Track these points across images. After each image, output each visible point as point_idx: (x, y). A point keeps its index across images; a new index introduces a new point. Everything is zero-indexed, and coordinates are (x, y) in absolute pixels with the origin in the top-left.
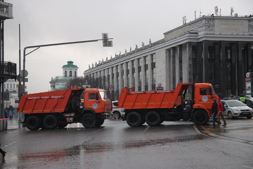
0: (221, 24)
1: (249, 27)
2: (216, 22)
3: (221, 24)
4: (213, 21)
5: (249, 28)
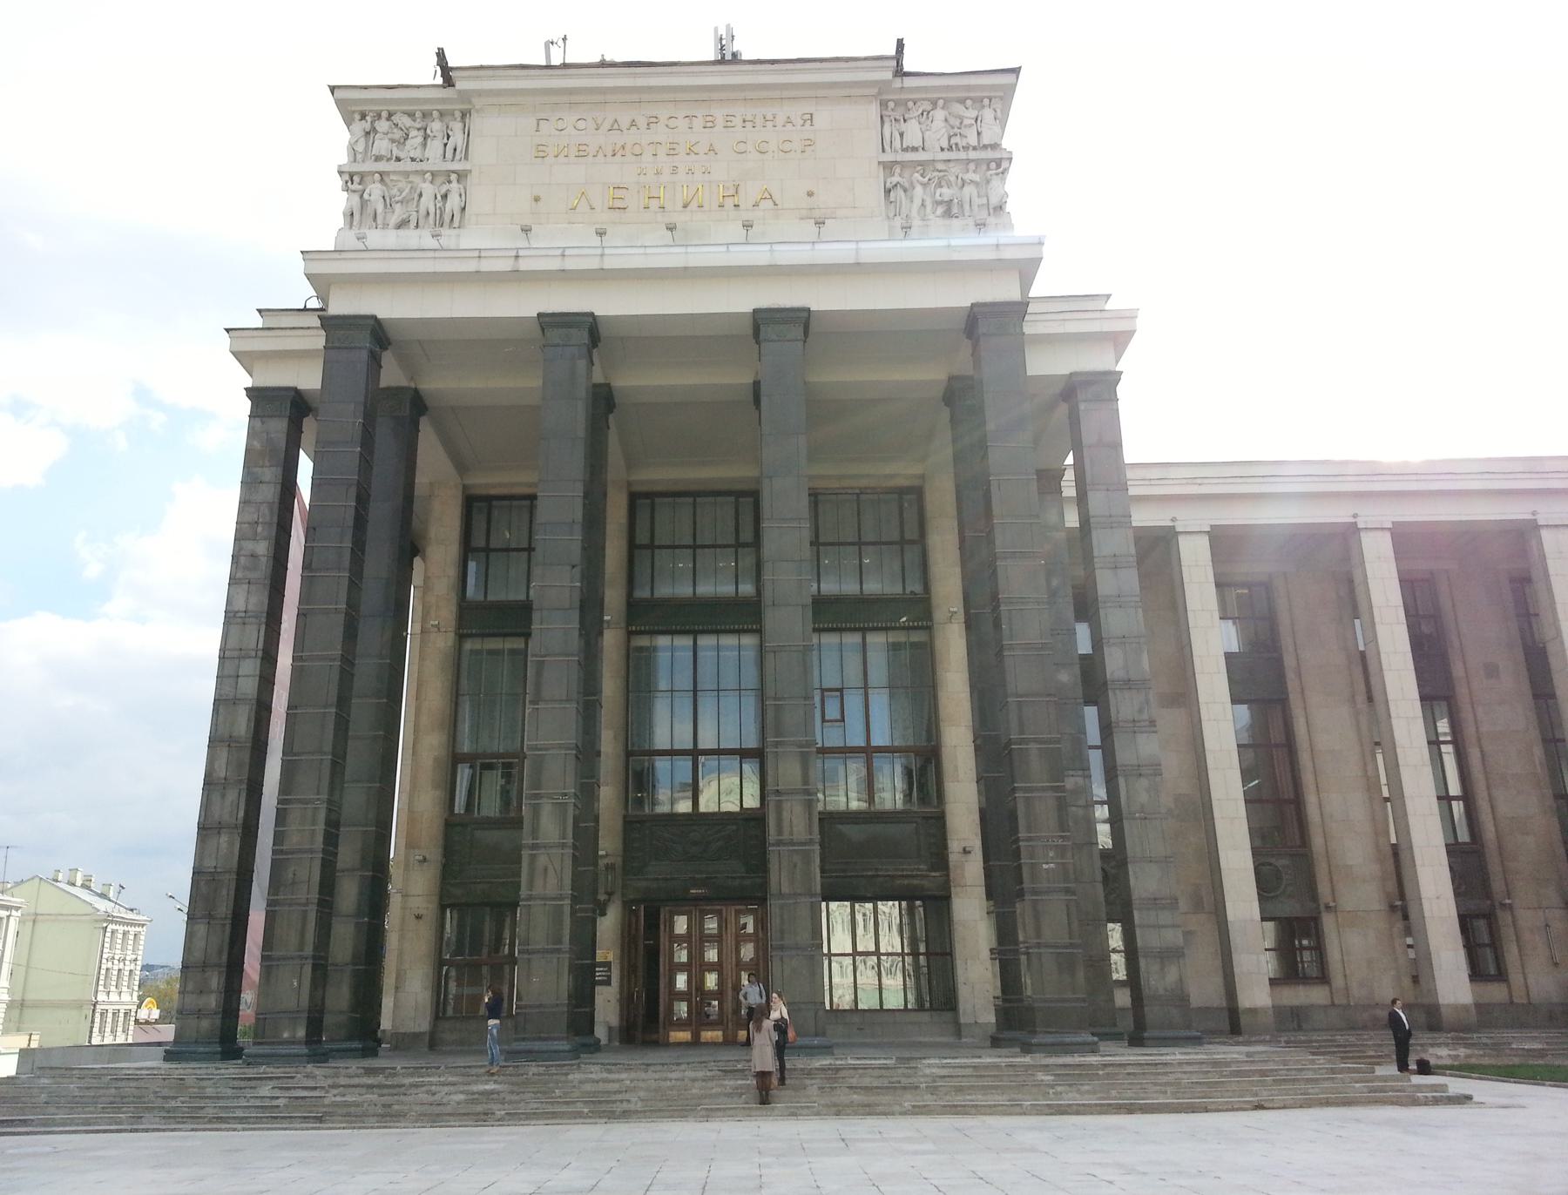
0: (540, 153)
1: (888, 167)
3: (540, 153)
4: (457, 126)
5: (896, 179)
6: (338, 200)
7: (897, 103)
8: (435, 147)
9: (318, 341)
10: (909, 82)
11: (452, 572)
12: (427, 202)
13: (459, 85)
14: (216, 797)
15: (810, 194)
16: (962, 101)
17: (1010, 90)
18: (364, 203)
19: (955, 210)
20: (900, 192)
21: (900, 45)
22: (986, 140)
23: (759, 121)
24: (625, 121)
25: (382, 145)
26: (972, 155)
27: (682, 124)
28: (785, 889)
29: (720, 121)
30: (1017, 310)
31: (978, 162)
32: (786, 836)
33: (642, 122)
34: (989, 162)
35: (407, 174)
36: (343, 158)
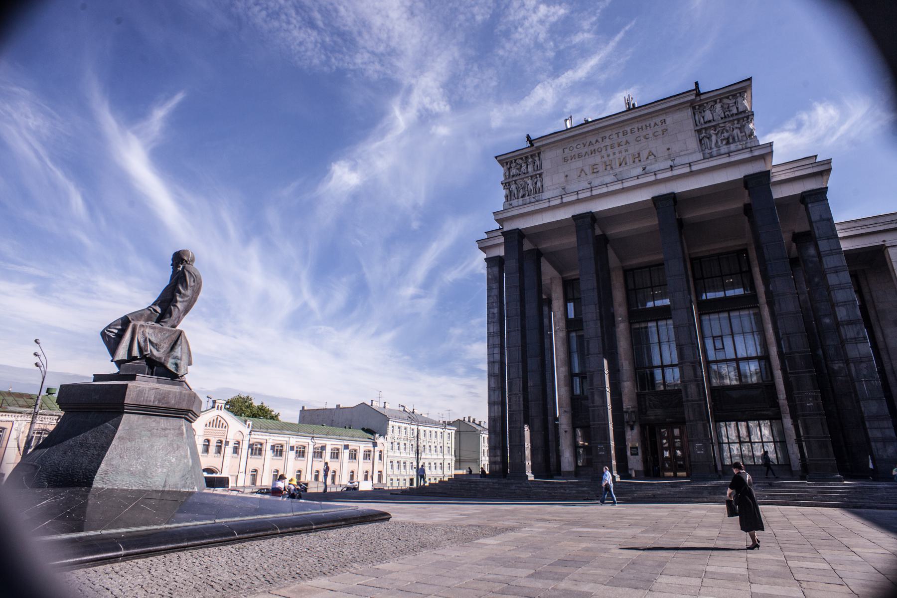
0: (565, 160)
2: (549, 159)
4: (537, 159)
6: (503, 192)
7: (700, 106)
8: (530, 168)
9: (501, 240)
10: (703, 97)
11: (562, 309)
12: (530, 187)
13: (536, 145)
14: (492, 393)
15: (668, 149)
16: (727, 98)
17: (750, 86)
18: (510, 192)
19: (731, 141)
20: (706, 140)
21: (697, 83)
22: (741, 109)
23: (644, 127)
24: (594, 141)
25: (514, 171)
26: (735, 117)
27: (615, 136)
28: (692, 418)
29: (629, 131)
30: (767, 174)
31: (738, 120)
32: (690, 398)
33: (600, 140)
34: (743, 118)
35: (522, 179)
36: (503, 179)
